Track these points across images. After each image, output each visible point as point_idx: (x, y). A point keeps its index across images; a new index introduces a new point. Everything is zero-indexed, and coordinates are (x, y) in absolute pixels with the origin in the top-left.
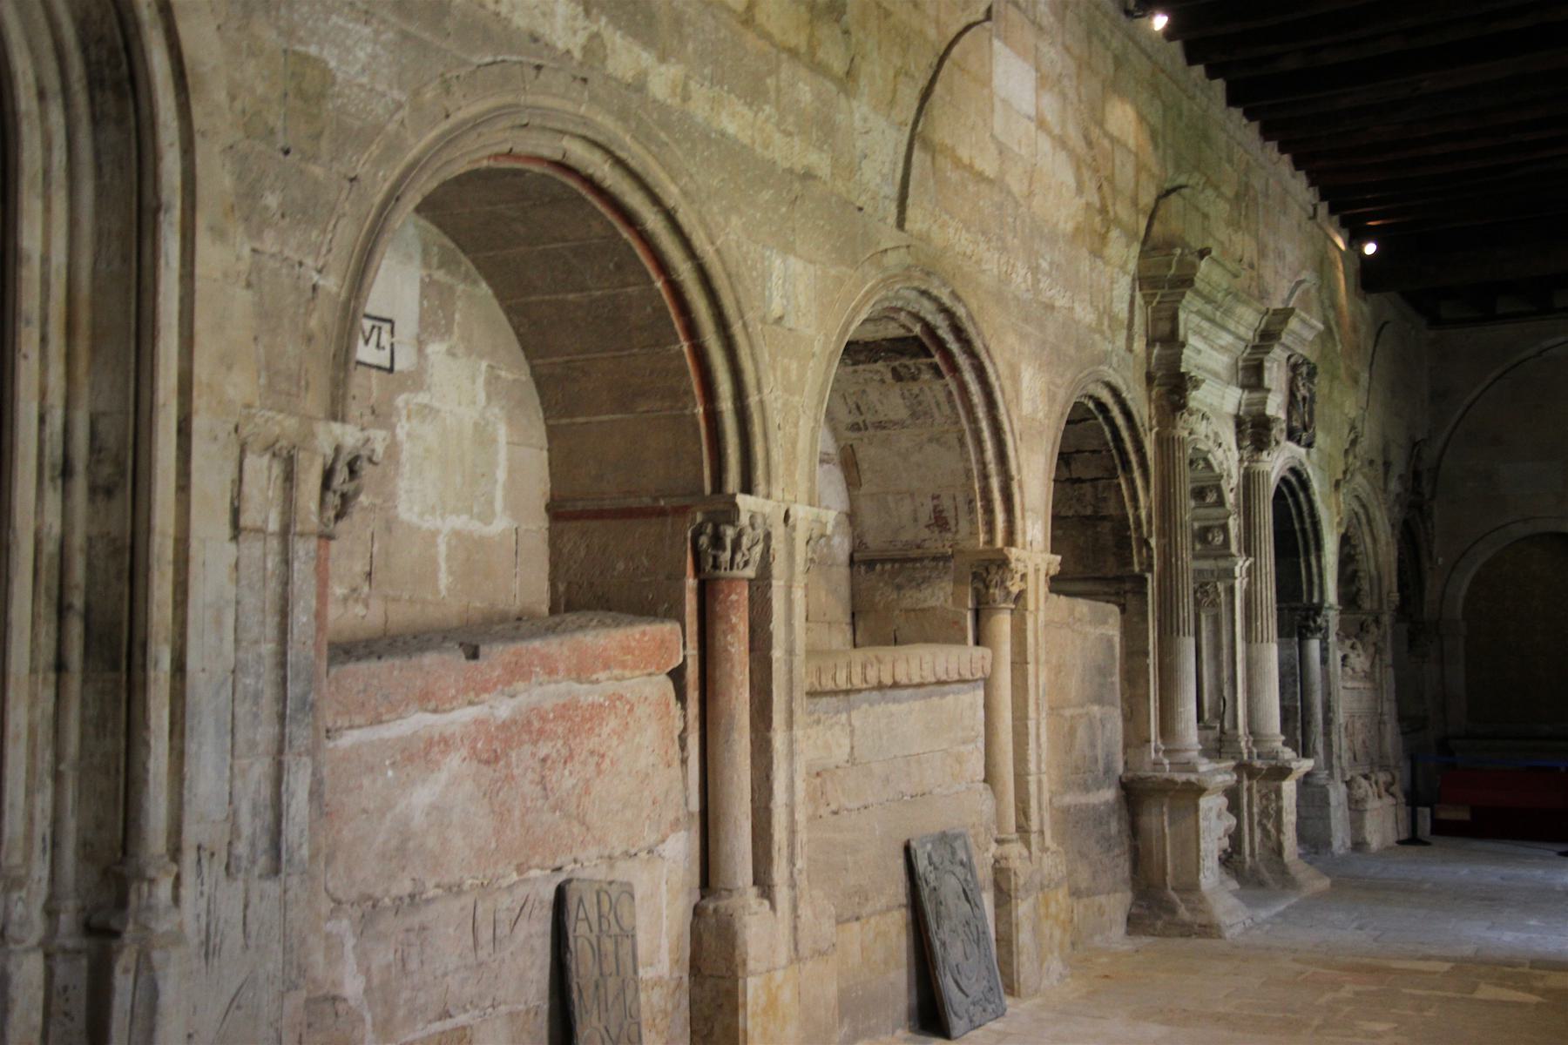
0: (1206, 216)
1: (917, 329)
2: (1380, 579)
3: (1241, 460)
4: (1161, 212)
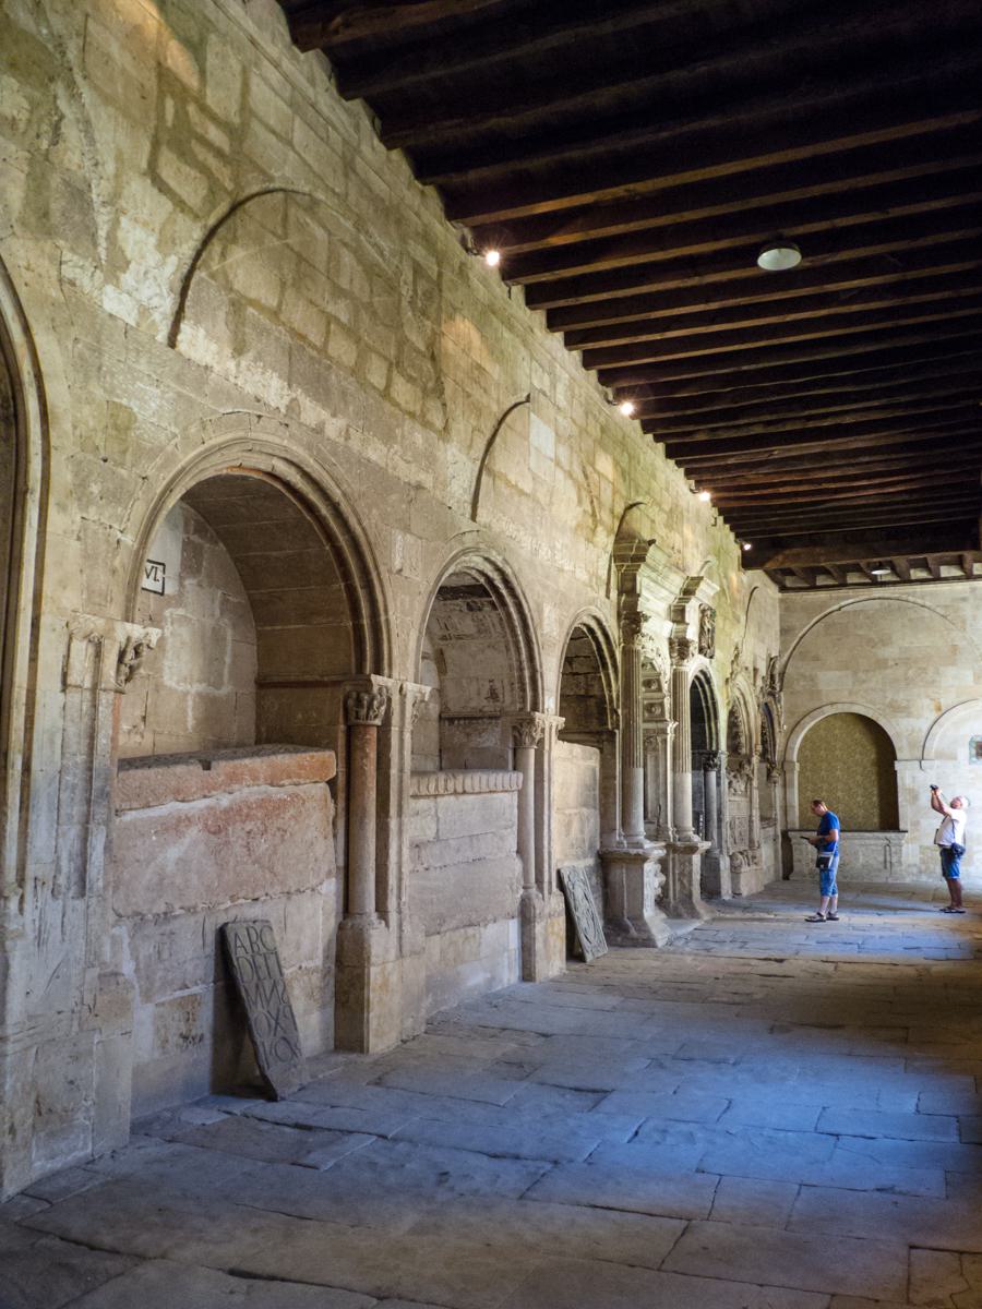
0: (653, 521)
1: (482, 580)
2: (751, 737)
3: (672, 665)
4: (627, 518)
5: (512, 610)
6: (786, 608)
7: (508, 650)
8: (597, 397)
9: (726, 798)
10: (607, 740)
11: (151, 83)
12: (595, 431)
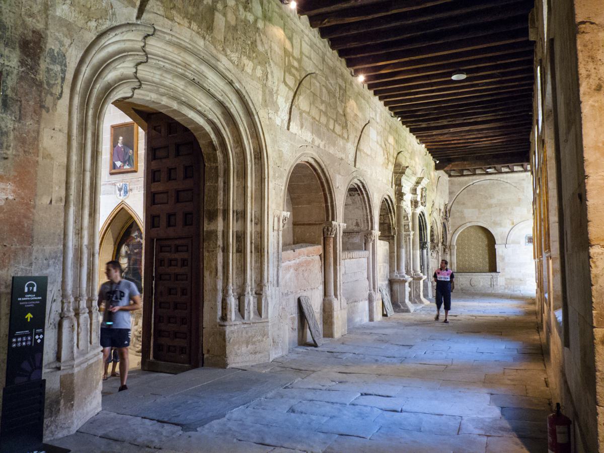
0: (406, 157)
1: (356, 186)
2: (438, 236)
4: (398, 158)
5: (365, 195)
6: (451, 184)
7: (363, 209)
8: (389, 116)
9: (430, 260)
10: (391, 239)
11: (283, 55)
12: (388, 128)
